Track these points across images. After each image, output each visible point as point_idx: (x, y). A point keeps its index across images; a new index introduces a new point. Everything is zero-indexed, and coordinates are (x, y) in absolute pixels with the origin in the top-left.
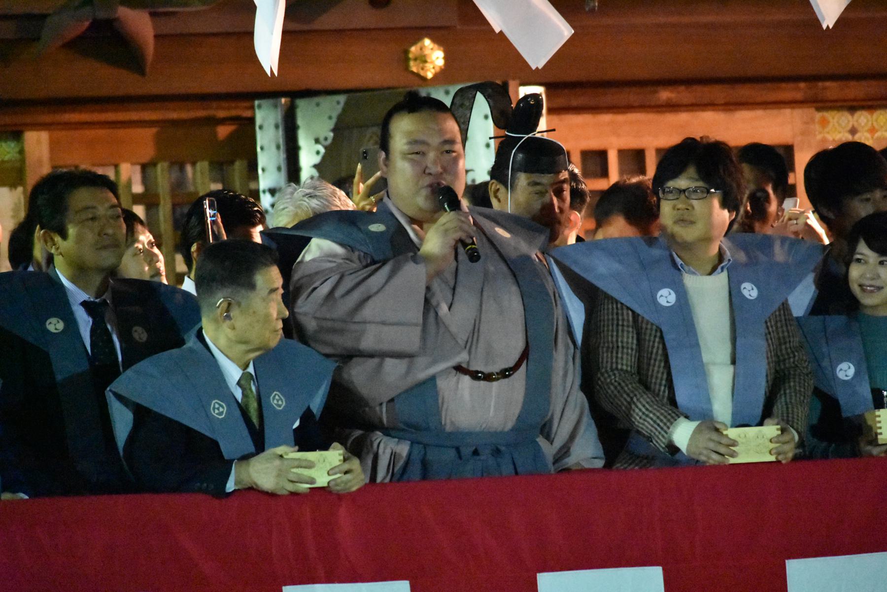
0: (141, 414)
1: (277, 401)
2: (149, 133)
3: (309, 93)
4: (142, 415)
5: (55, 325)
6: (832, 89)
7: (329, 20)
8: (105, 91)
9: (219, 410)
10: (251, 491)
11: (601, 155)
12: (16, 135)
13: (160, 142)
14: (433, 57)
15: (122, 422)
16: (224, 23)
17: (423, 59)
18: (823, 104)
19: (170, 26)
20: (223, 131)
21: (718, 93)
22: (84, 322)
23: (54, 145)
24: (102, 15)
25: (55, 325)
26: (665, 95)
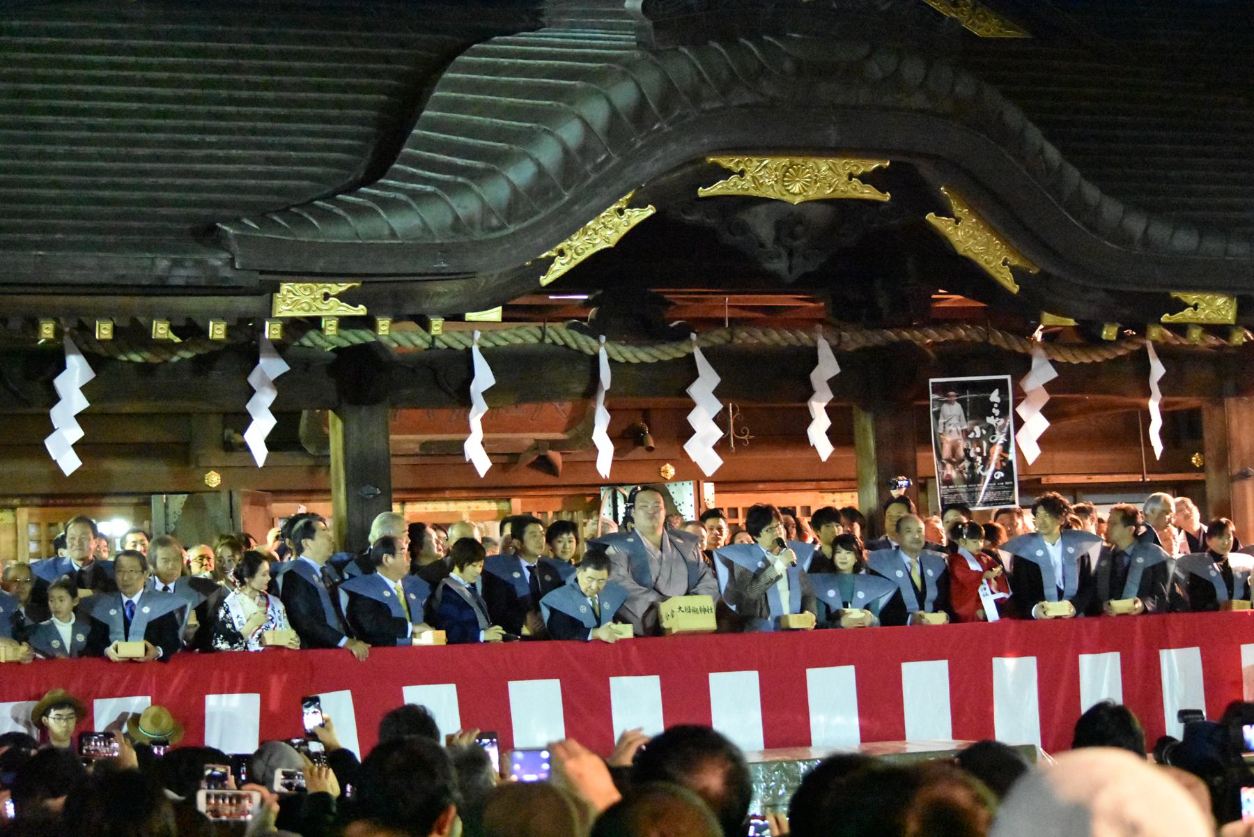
0: (553, 611)
1: (606, 606)
2: (559, 500)
3: (622, 485)
4: (553, 611)
5: (517, 575)
6: (825, 484)
7: (631, 456)
8: (543, 483)
9: (583, 609)
10: (598, 641)
11: (736, 509)
12: (508, 500)
13: (564, 503)
14: (670, 471)
15: (546, 614)
16: (588, 458)
17: (666, 472)
18: (822, 490)
19: (570, 458)
20: (589, 499)
21: (781, 486)
22: (527, 574)
23: (523, 504)
24: (542, 454)
25: (517, 575)
26: (761, 486)
